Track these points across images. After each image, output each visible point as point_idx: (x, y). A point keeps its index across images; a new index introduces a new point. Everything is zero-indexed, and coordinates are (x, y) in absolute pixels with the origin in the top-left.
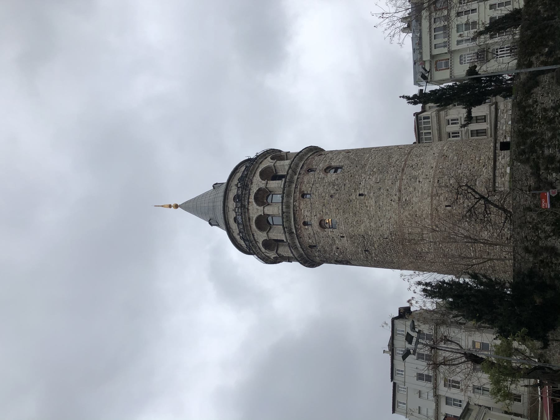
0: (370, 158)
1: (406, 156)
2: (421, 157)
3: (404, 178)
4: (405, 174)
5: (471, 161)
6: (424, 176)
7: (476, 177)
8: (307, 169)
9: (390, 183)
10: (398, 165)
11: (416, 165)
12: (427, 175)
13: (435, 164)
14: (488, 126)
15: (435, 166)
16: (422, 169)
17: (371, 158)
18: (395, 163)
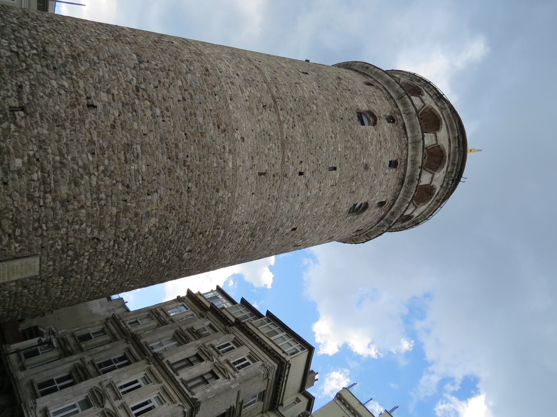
0: (334, 139)
1: (285, 137)
2: (261, 132)
3: (265, 85)
4: (267, 91)
5: (167, 105)
6: (237, 84)
7: (142, 66)
8: (396, 122)
9: (279, 79)
10: (287, 113)
11: (260, 111)
12: (232, 83)
13: (231, 107)
14: (177, 378)
15: (229, 101)
16: (247, 98)
17: (331, 137)
18: (293, 118)
